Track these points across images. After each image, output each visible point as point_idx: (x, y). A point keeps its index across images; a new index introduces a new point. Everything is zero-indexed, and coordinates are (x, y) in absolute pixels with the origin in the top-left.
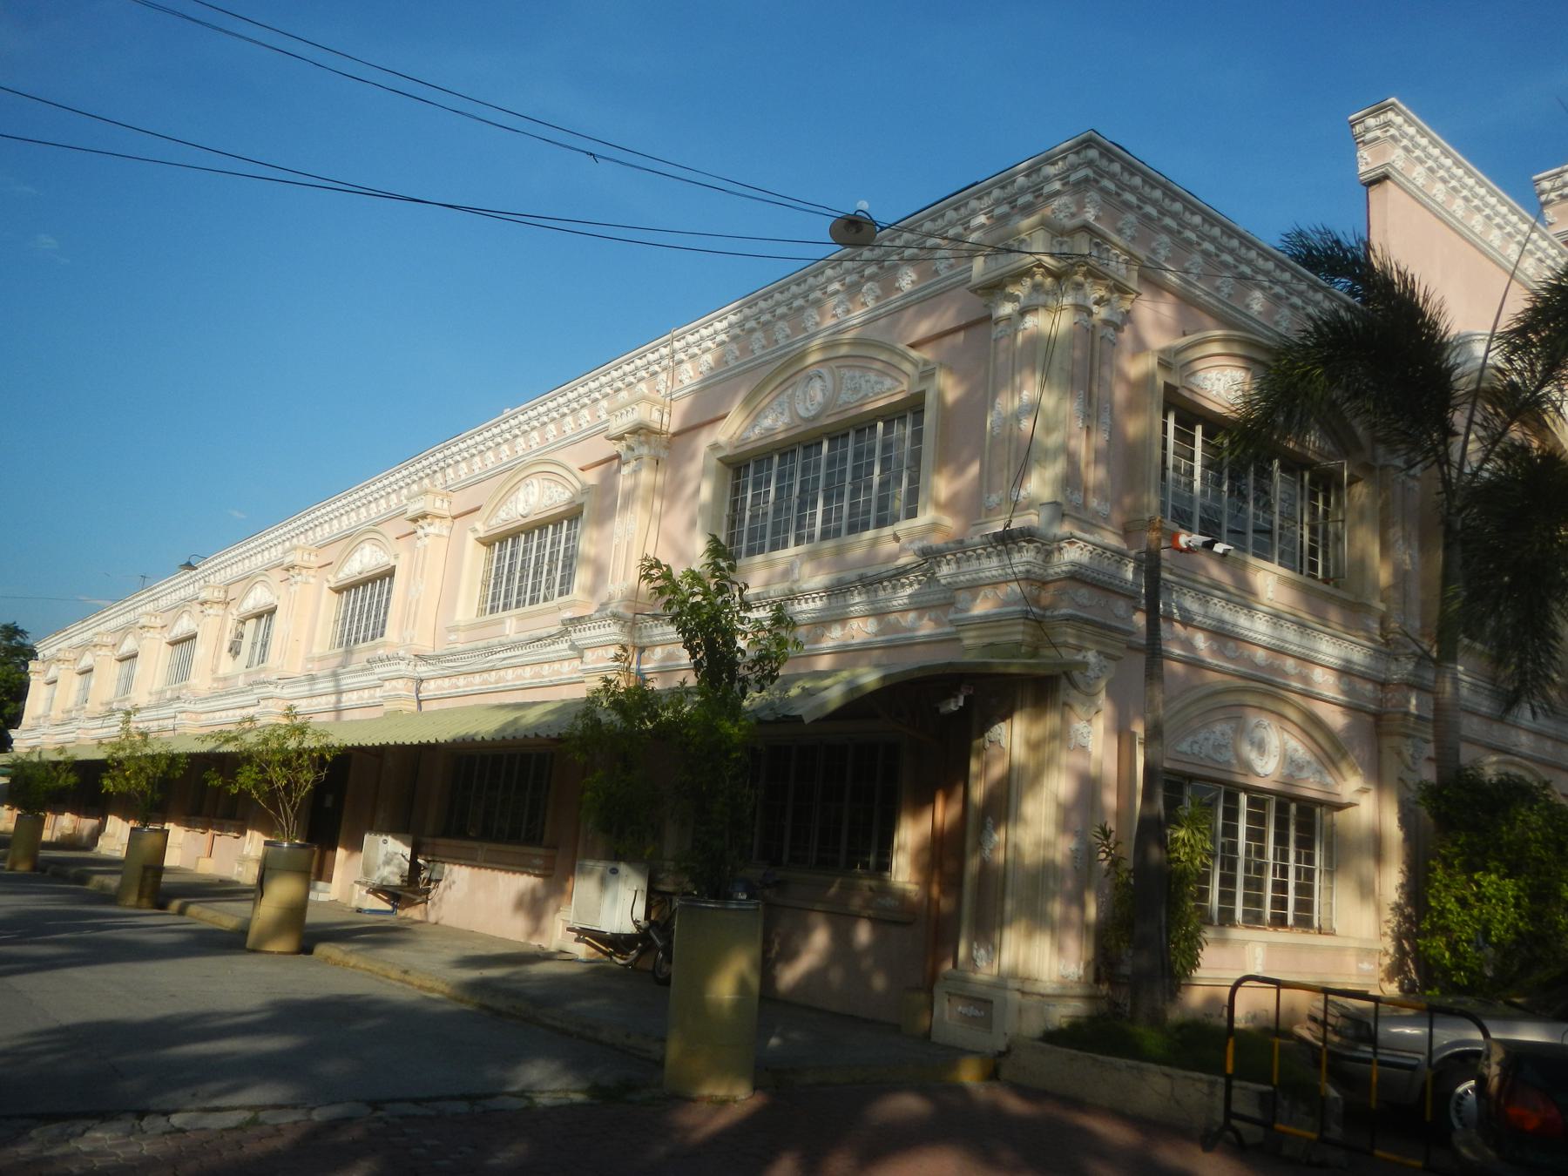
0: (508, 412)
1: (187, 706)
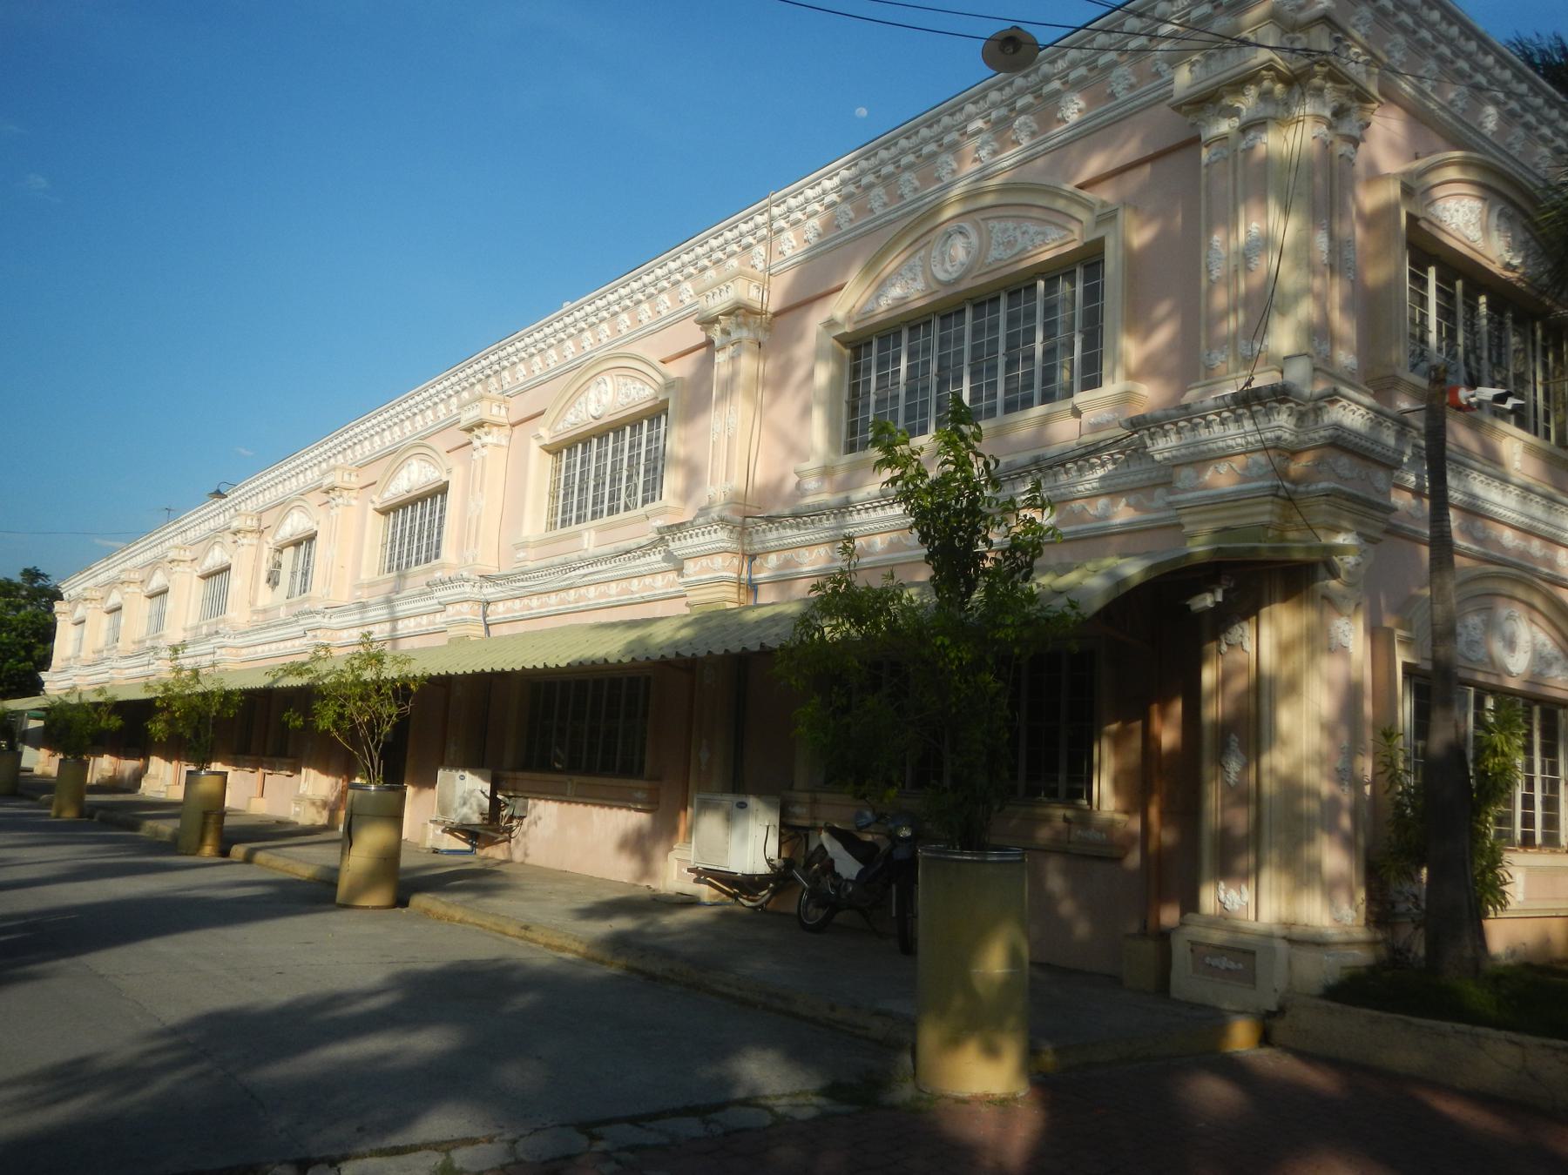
0: (567, 306)
1: (226, 641)
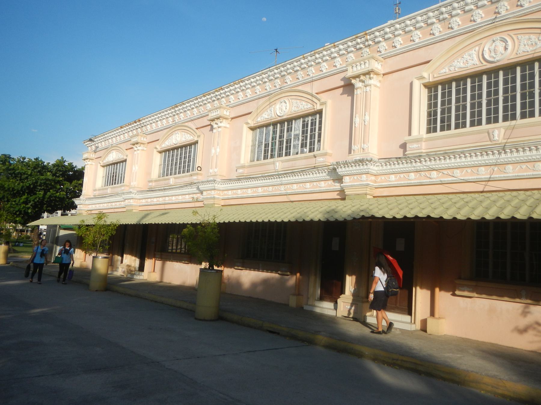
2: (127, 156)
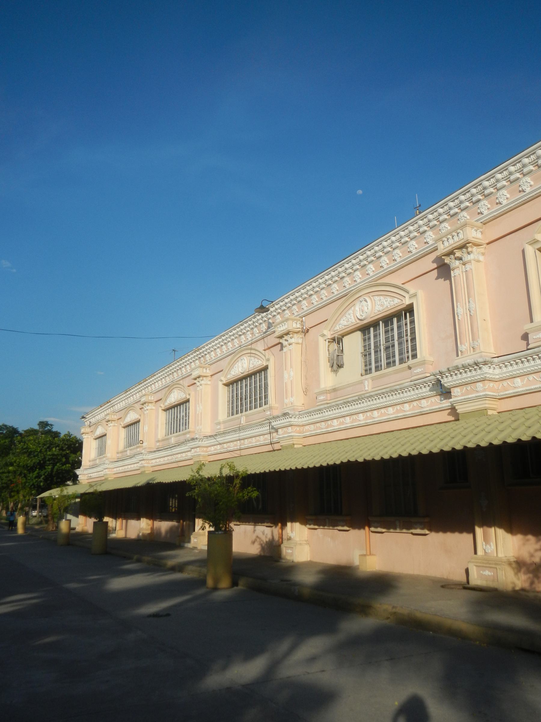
1: (294, 421)
2: (268, 360)
